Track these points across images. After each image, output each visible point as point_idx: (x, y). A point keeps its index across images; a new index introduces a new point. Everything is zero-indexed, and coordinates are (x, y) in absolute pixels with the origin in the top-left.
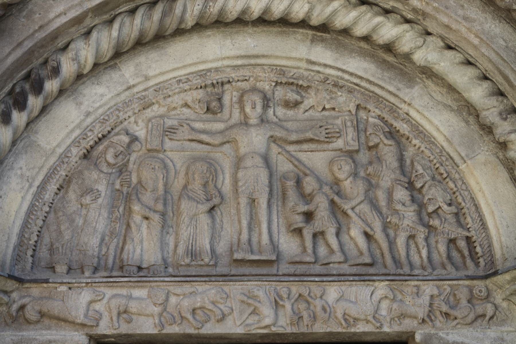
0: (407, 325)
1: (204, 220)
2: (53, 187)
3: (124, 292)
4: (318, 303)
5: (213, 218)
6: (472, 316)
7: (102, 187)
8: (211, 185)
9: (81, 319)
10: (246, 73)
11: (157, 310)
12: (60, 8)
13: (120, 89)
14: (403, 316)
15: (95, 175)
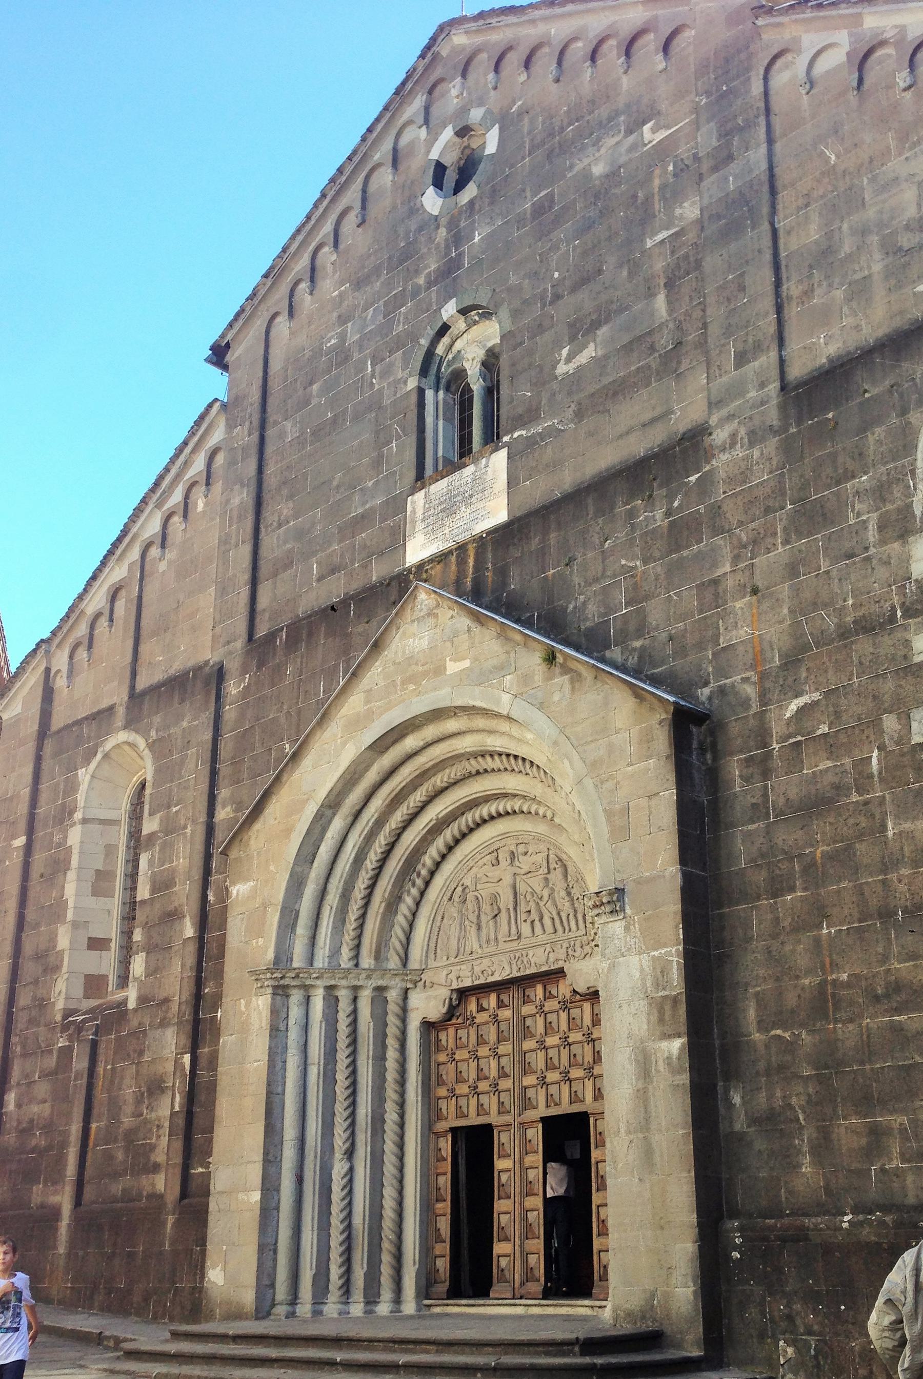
0: (560, 964)
1: (491, 923)
2: (439, 918)
3: (458, 967)
4: (525, 960)
5: (496, 922)
6: (583, 955)
7: (456, 915)
8: (494, 905)
9: (444, 983)
10: (503, 843)
11: (470, 974)
12: (412, 838)
13: (456, 863)
14: (557, 960)
15: (453, 909)
